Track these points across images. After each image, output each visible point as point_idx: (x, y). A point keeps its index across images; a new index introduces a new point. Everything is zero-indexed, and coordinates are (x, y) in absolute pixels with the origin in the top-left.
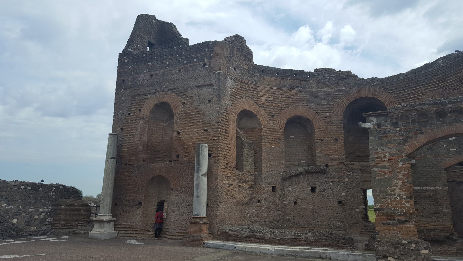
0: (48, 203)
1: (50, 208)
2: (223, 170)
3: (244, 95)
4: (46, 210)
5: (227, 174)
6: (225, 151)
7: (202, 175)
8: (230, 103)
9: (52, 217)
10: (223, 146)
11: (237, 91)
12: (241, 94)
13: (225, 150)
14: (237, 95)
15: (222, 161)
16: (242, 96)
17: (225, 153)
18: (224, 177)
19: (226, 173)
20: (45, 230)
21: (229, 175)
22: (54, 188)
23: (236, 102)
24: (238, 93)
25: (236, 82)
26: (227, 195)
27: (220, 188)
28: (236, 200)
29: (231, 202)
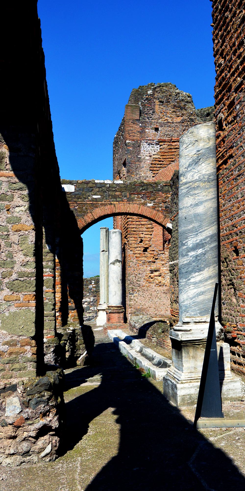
0: (90, 294)
1: (92, 298)
2: (138, 255)
3: (177, 157)
4: (89, 300)
5: (145, 259)
6: (143, 234)
7: (111, 264)
8: (150, 174)
9: (95, 306)
10: (136, 228)
11: (162, 156)
12: (170, 158)
13: (141, 233)
14: (163, 162)
15: (136, 246)
16: (173, 160)
17: (142, 236)
18: (139, 263)
19: (144, 258)
20: (89, 317)
21: (152, 259)
22: (94, 281)
23: (162, 170)
24: (164, 158)
25: (160, 146)
26: (150, 282)
27: (134, 275)
28: (166, 288)
29: (156, 291)
